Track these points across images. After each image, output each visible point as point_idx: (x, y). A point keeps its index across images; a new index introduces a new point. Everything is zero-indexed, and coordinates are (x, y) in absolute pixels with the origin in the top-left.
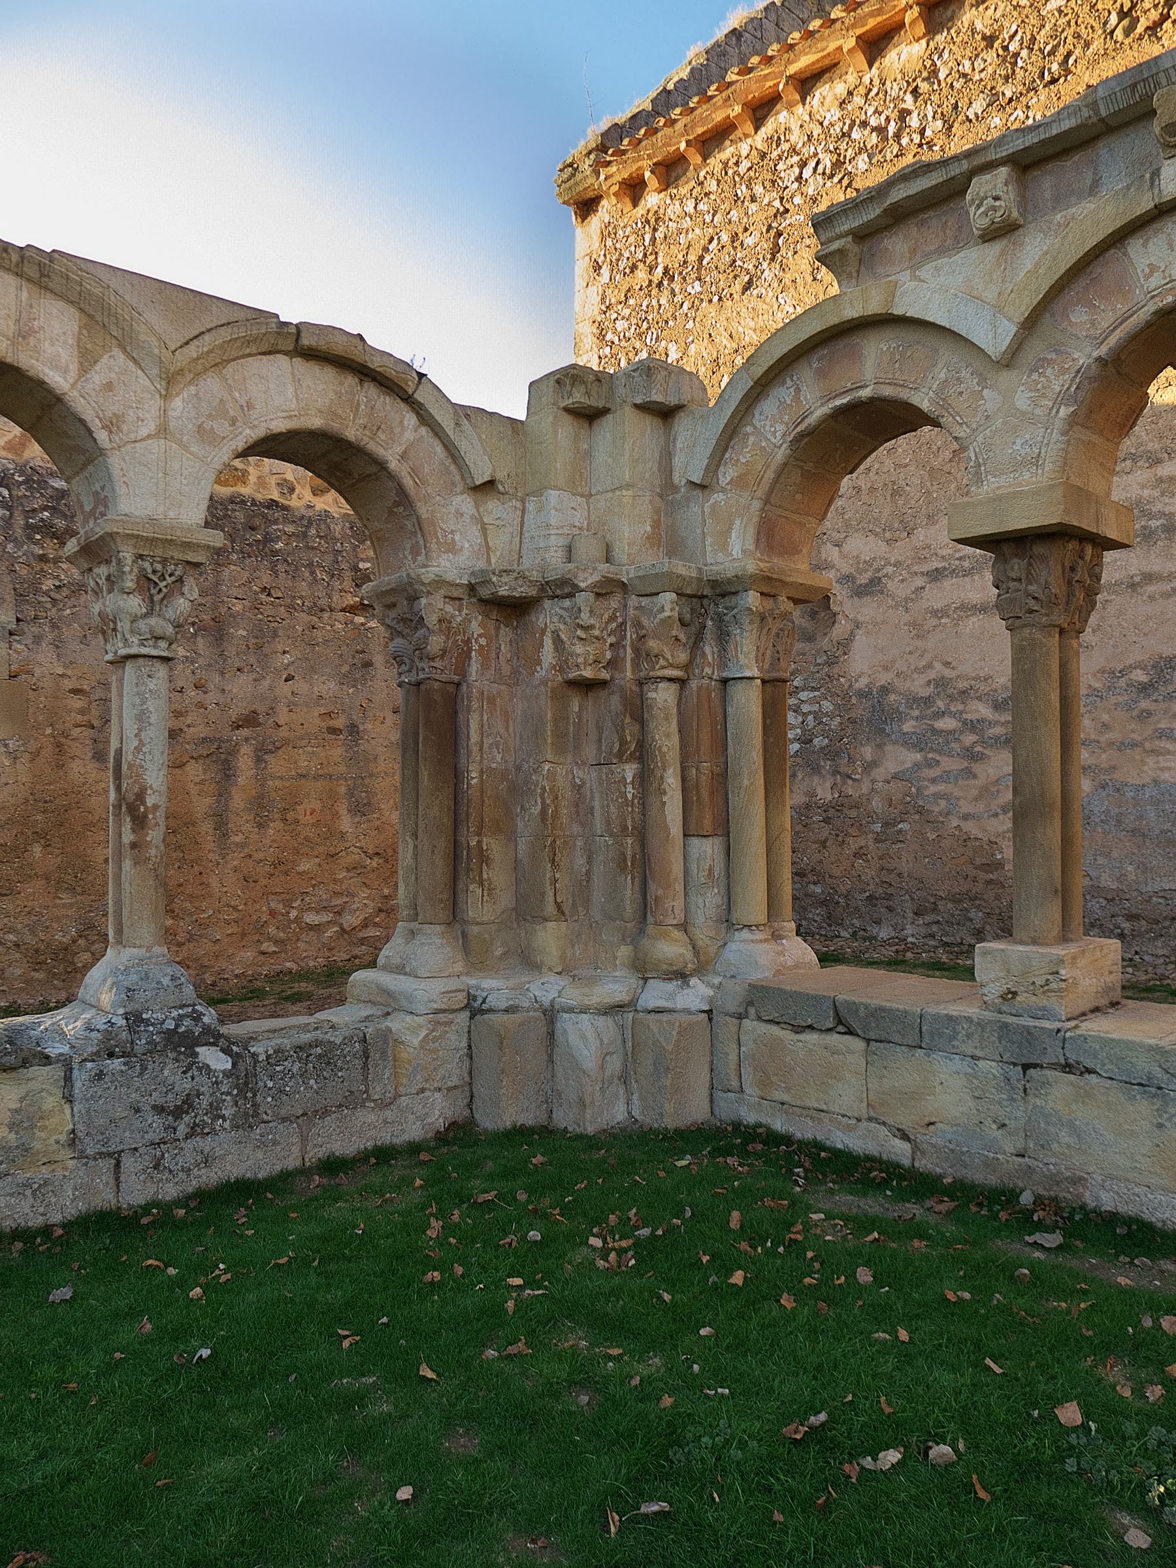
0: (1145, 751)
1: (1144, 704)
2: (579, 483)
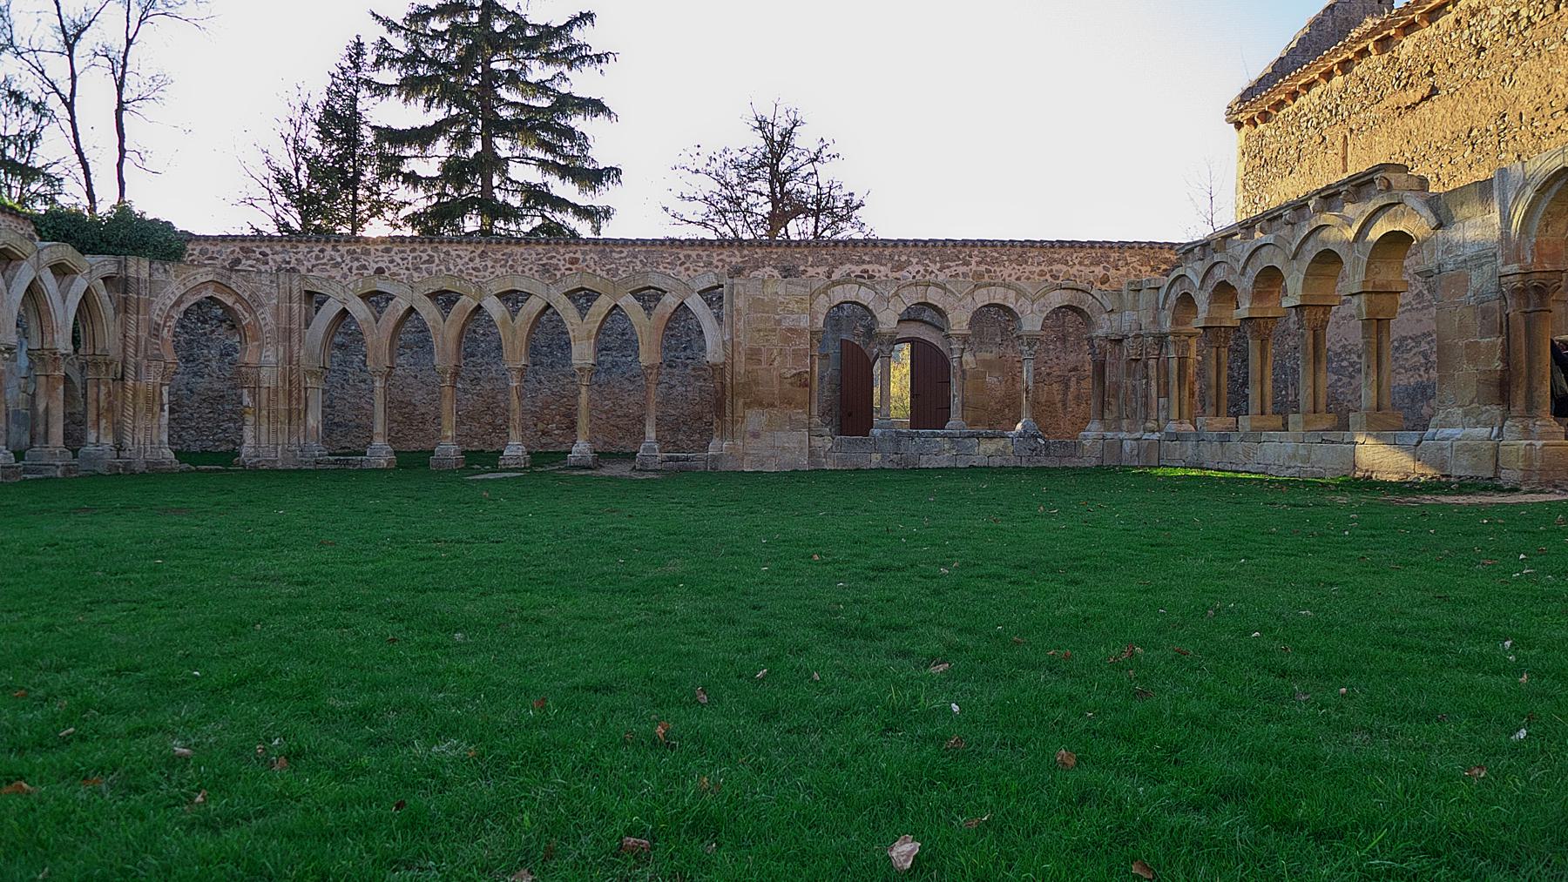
2: (1135, 308)
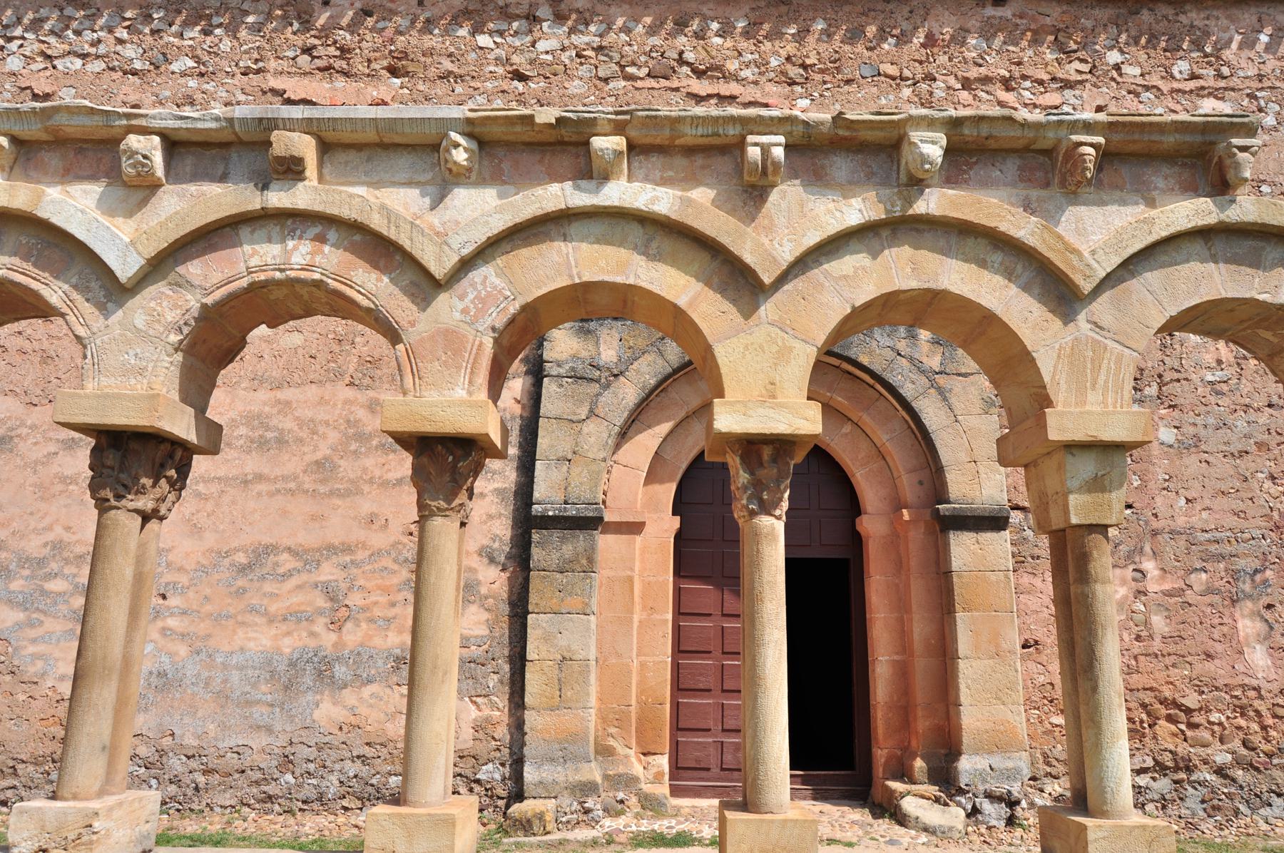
0: (237, 622)
1: (240, 583)
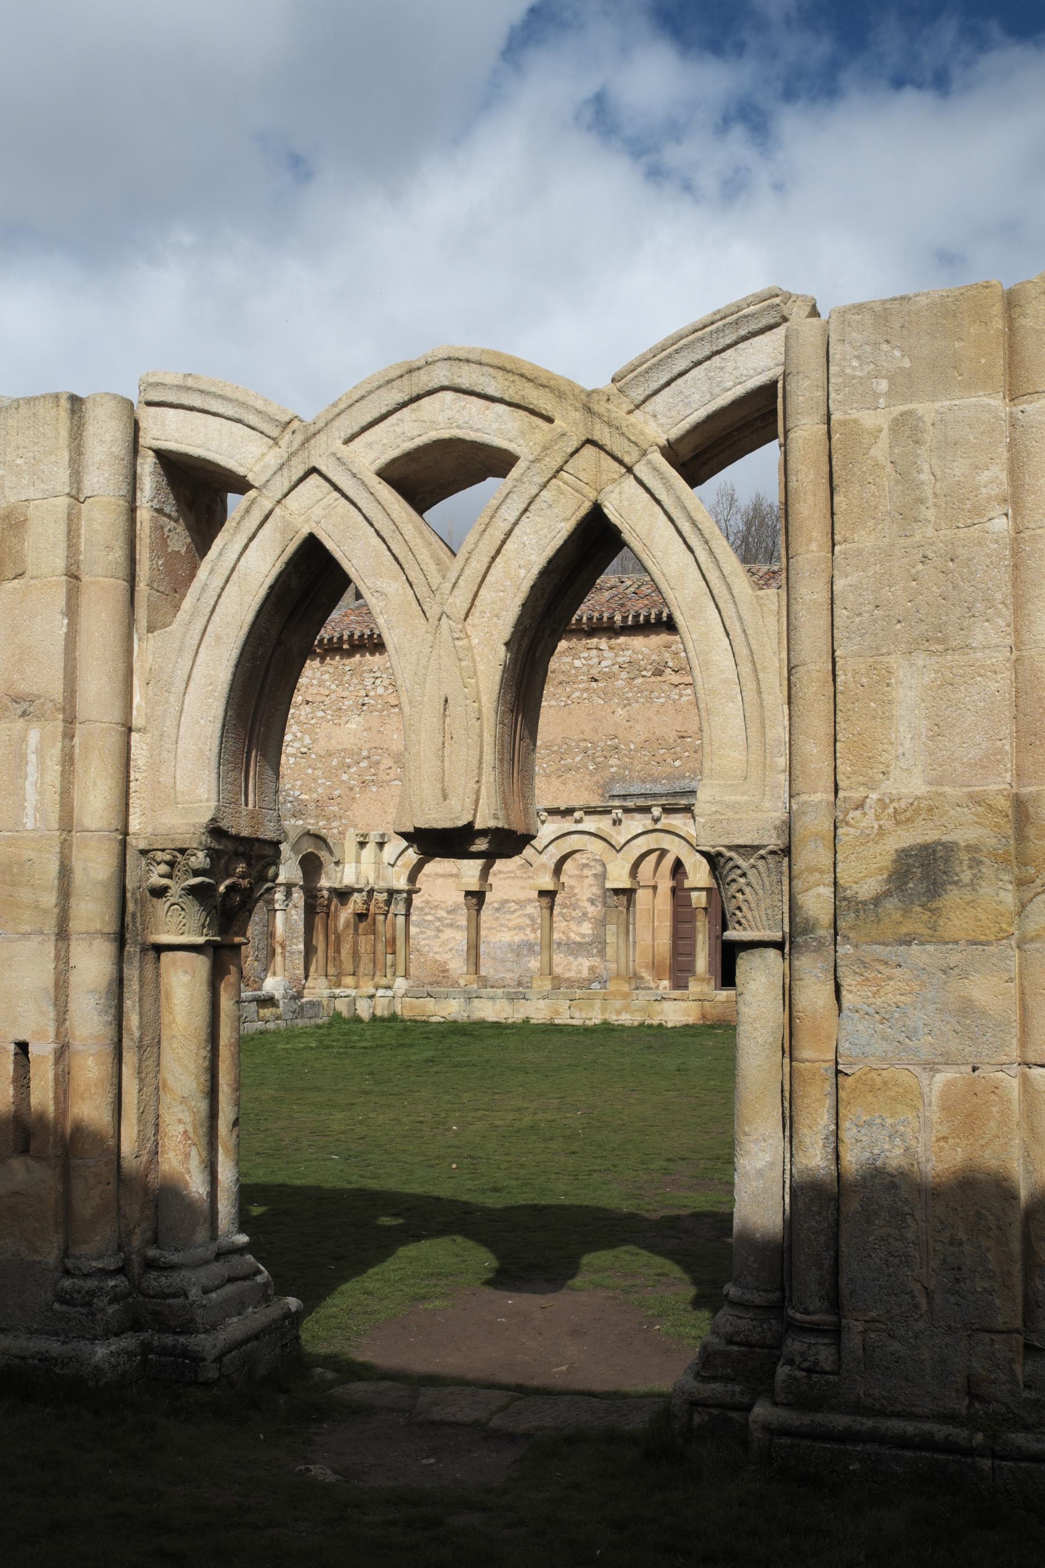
1: (497, 915)
